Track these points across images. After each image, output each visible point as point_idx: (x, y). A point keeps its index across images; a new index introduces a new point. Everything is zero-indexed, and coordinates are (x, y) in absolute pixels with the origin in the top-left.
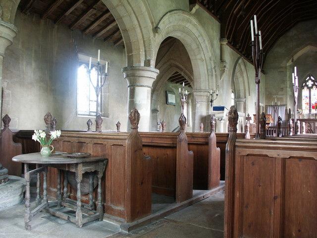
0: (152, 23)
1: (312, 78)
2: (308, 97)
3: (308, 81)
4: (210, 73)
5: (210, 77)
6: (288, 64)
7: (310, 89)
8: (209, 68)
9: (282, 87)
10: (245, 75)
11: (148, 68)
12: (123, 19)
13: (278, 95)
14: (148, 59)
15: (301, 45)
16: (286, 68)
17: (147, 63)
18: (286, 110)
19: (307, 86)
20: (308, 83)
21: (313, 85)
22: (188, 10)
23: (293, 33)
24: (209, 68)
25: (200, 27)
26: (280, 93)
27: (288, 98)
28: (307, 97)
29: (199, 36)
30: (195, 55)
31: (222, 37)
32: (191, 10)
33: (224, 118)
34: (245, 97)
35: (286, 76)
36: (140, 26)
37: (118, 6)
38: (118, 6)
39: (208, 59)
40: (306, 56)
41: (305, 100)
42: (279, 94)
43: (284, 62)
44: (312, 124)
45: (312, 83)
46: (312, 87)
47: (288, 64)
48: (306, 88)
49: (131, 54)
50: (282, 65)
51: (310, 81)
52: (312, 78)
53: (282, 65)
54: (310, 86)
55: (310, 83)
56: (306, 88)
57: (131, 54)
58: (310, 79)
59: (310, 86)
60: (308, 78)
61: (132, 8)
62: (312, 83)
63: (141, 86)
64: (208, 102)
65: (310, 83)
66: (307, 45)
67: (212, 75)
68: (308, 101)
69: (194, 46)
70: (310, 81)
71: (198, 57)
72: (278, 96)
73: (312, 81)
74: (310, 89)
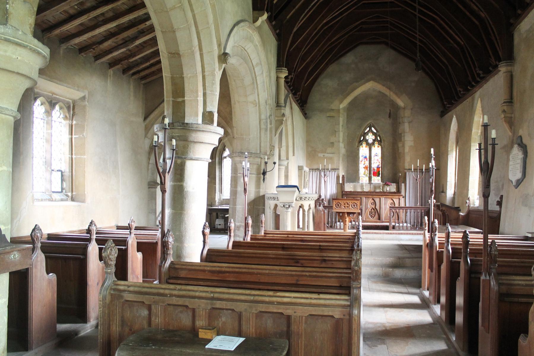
0: (219, 45)
1: (373, 129)
2: (368, 157)
3: (367, 134)
4: (263, 126)
5: (263, 132)
6: (341, 106)
7: (370, 146)
8: (263, 117)
9: (332, 141)
10: (289, 122)
11: (209, 127)
12: (179, 34)
13: (325, 153)
14: (208, 109)
15: (361, 78)
16: (338, 111)
17: (208, 118)
18: (338, 177)
19: (367, 141)
20: (367, 137)
21: (374, 141)
22: (251, 20)
23: (349, 59)
24: (263, 117)
25: (260, 49)
26: (329, 150)
27: (341, 159)
28: (365, 158)
29: (257, 65)
30: (246, 96)
31: (279, 65)
32: (255, 20)
33: (293, 205)
34: (288, 159)
35: (339, 124)
36: (201, 49)
37: (174, 8)
38: (174, 8)
39: (262, 102)
40: (366, 96)
41: (363, 163)
42: (328, 151)
43: (336, 102)
44: (377, 200)
45: (373, 137)
46: (373, 144)
47: (341, 106)
48: (364, 145)
49: (180, 100)
50: (334, 106)
51: (370, 134)
52: (373, 129)
53: (334, 106)
54: (370, 141)
55: (370, 138)
56: (364, 145)
57: (180, 100)
58: (370, 130)
59: (370, 141)
60: (368, 129)
61: (194, 16)
62: (373, 137)
63: (191, 159)
64: (258, 174)
65: (370, 138)
66: (368, 81)
67: (266, 130)
68: (367, 163)
69: (248, 80)
70: (370, 134)
71: (251, 98)
72: (326, 155)
73: (374, 133)
74: (370, 146)
